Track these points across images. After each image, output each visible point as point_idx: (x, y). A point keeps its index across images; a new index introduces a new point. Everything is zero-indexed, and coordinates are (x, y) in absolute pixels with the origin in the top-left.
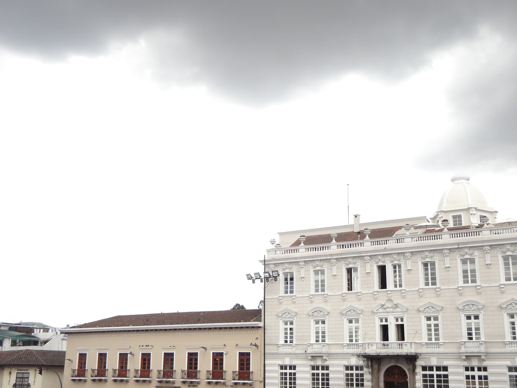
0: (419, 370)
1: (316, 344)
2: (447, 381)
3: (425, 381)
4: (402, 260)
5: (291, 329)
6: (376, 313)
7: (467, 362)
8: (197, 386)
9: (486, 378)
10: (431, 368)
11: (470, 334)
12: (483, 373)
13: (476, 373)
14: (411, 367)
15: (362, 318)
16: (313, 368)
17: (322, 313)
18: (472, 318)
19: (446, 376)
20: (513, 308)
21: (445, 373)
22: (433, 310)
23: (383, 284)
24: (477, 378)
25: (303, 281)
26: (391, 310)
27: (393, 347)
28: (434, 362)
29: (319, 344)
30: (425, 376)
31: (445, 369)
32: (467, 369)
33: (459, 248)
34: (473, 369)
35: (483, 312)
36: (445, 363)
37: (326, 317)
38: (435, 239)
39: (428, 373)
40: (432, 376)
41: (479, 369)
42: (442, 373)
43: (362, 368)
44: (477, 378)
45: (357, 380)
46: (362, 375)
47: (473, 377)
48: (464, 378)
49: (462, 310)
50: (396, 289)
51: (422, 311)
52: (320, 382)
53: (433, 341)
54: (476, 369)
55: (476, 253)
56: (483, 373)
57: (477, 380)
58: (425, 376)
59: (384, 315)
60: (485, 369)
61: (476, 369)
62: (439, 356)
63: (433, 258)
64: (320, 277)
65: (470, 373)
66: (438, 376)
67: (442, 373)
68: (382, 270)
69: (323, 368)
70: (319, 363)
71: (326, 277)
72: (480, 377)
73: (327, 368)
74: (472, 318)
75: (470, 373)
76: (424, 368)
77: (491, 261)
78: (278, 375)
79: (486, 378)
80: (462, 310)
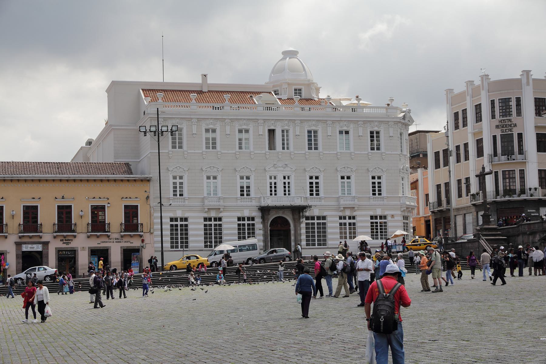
0: (304, 220)
1: (402, 197)
2: (325, 228)
3: (307, 228)
4: (291, 126)
5: (289, 183)
6: (268, 171)
7: (207, 214)
8: (72, 240)
9: (354, 224)
10: (313, 218)
11: (242, 191)
12: (352, 221)
13: (347, 221)
14: (297, 217)
15: (221, 175)
16: (205, 219)
17: (215, 169)
18: (212, 178)
19: (324, 224)
20: (177, 171)
21: (186, 223)
22: (317, 170)
23: (272, 146)
24: (347, 224)
25: (194, 137)
26: (282, 169)
27: (283, 200)
28: (316, 212)
29: (211, 197)
30: (307, 224)
31: (324, 218)
32: (340, 218)
33: (341, 120)
34: (345, 218)
35: (323, 174)
36: (325, 214)
37: (322, 173)
38: (269, 110)
39: (208, 223)
40: (313, 224)
41: (350, 218)
42: (321, 221)
43: (253, 219)
44: (347, 224)
45: (215, 230)
46: (253, 225)
47: (345, 224)
48: (236, 226)
49: (339, 172)
50: (284, 151)
51: (308, 171)
52: (179, 232)
53: (346, 195)
54: (347, 218)
55: (352, 126)
56: (352, 221)
57: (348, 226)
58: (307, 224)
59: (273, 174)
60: (354, 218)
61: (347, 218)
62: (184, 209)
63: (318, 127)
64: (211, 135)
65: (343, 221)
66: (318, 224)
67: (321, 221)
68: (272, 132)
69: (215, 219)
70: (213, 214)
71: (218, 135)
72: (350, 224)
73: (220, 219)
74: (212, 178)
75: (343, 221)
76: (307, 218)
77: (331, 133)
78: (169, 227)
79: (354, 224)
80: (339, 172)
